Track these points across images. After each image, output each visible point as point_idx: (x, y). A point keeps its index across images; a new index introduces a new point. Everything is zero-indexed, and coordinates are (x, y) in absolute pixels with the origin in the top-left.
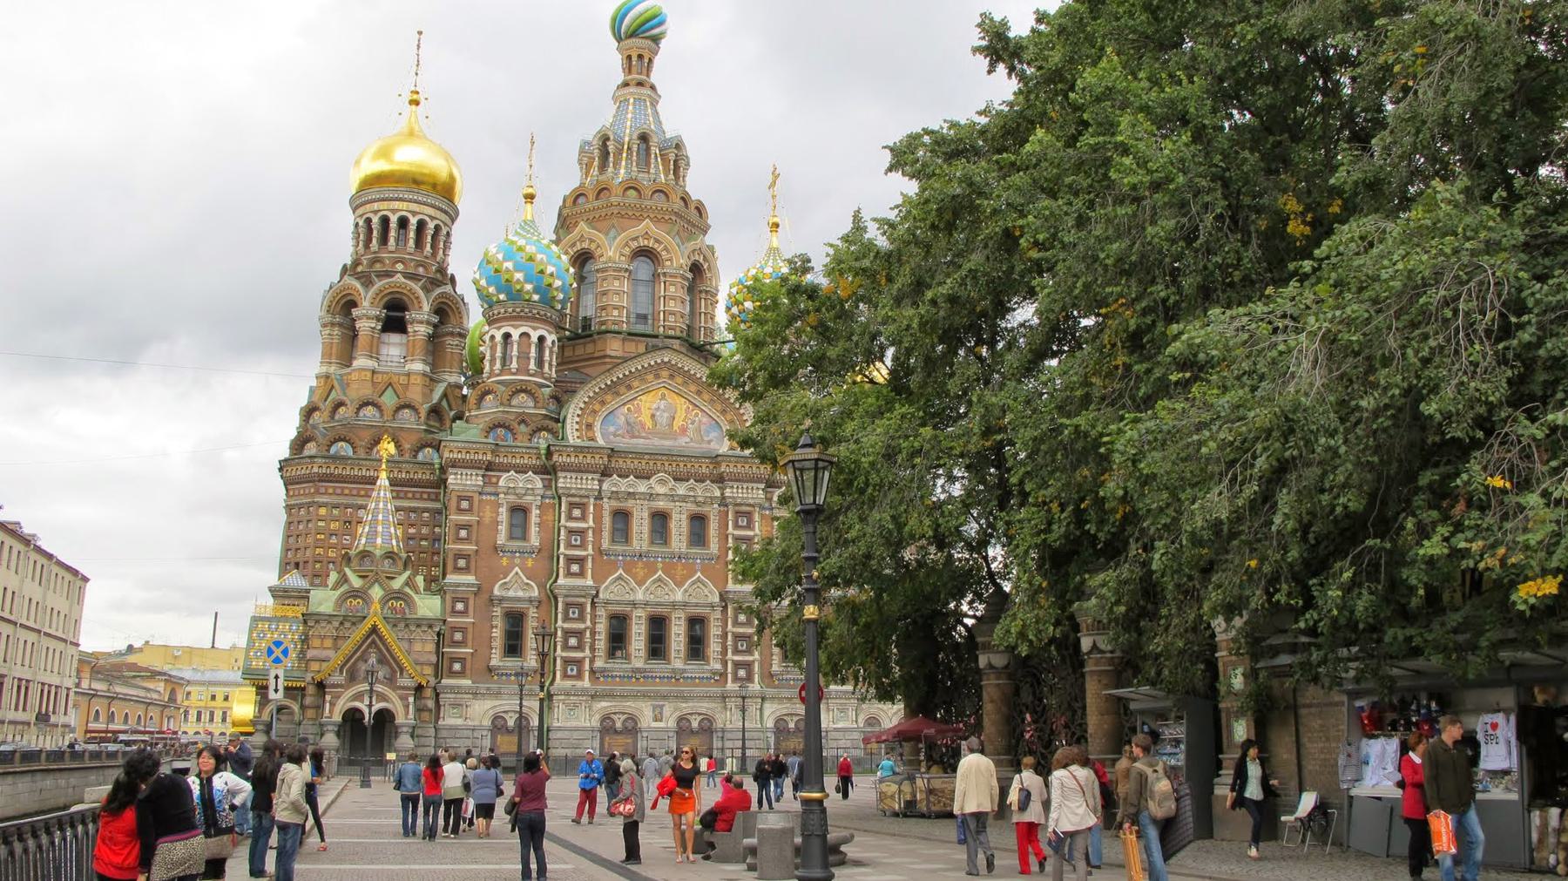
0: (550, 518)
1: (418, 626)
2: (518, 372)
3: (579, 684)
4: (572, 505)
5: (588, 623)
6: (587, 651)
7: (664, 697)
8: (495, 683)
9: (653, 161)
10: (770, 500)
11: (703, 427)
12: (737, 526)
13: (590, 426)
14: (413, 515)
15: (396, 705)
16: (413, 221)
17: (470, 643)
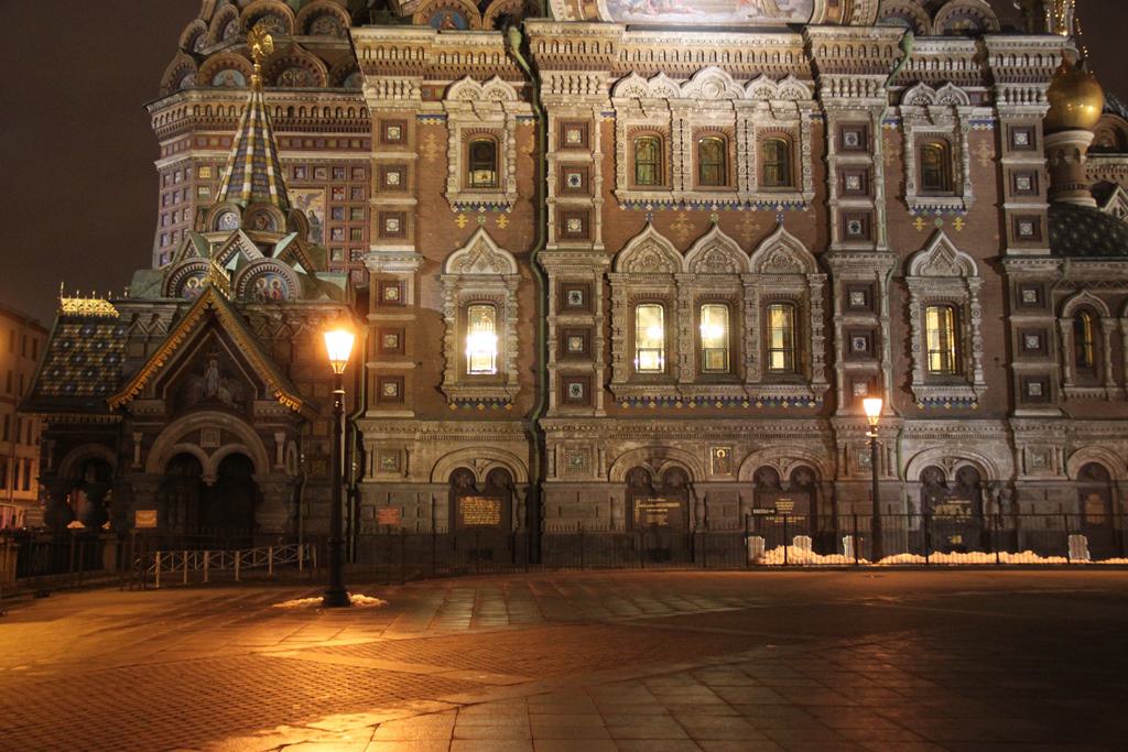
5: (600, 313)
12: (842, 148)
15: (252, 444)
17: (410, 352)
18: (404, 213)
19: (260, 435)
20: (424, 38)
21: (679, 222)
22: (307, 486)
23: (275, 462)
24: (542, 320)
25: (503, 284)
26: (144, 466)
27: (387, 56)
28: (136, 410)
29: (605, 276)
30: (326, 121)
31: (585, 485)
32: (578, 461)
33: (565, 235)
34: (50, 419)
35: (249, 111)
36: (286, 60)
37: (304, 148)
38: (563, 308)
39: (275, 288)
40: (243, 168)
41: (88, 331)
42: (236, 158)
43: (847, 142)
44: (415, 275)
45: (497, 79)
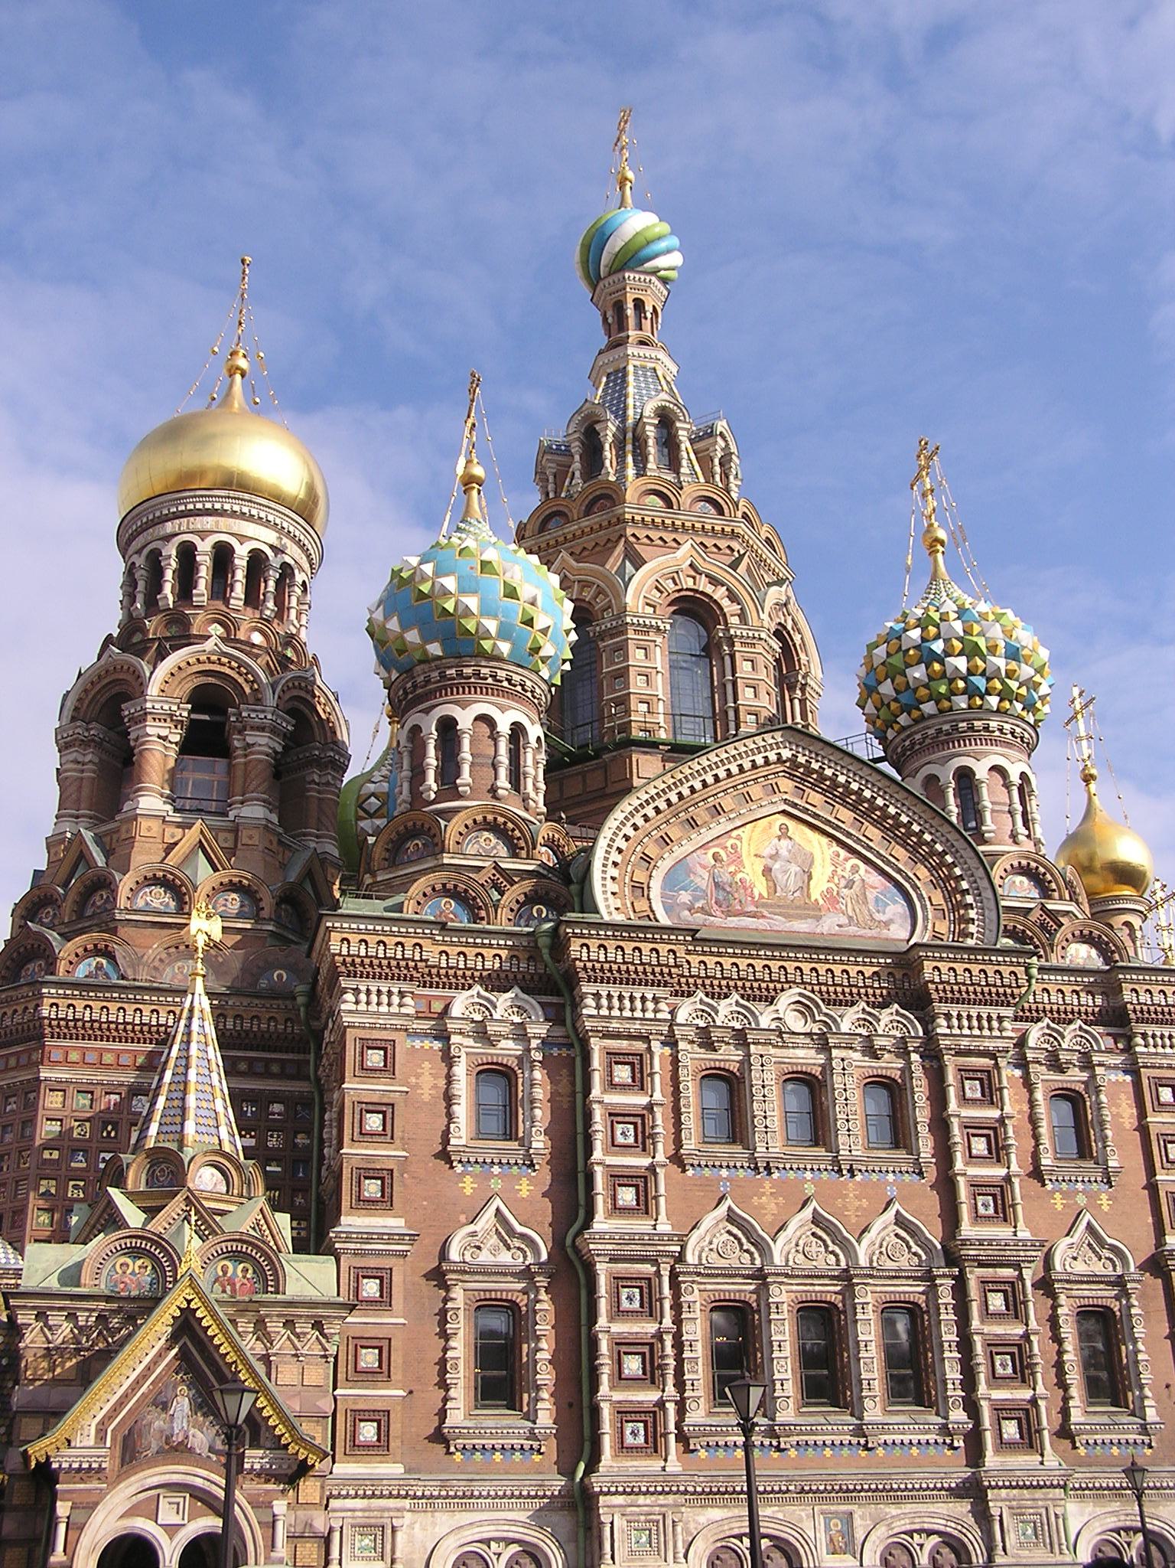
0: (564, 1087)
1: (289, 1324)
2: (474, 794)
3: (656, 1465)
4: (614, 1058)
5: (668, 1322)
6: (670, 1389)
7: (848, 1493)
8: (460, 1468)
9: (684, 454)
10: (1021, 1042)
11: (871, 895)
12: (964, 1100)
13: (640, 889)
14: (249, 1110)
16: (242, 552)
17: (396, 1375)
18: (392, 1170)
21: (763, 1194)
23: (273, 1546)
24: (584, 1330)
29: (673, 1268)
35: (190, 1018)
39: (244, 1277)
43: (969, 1094)
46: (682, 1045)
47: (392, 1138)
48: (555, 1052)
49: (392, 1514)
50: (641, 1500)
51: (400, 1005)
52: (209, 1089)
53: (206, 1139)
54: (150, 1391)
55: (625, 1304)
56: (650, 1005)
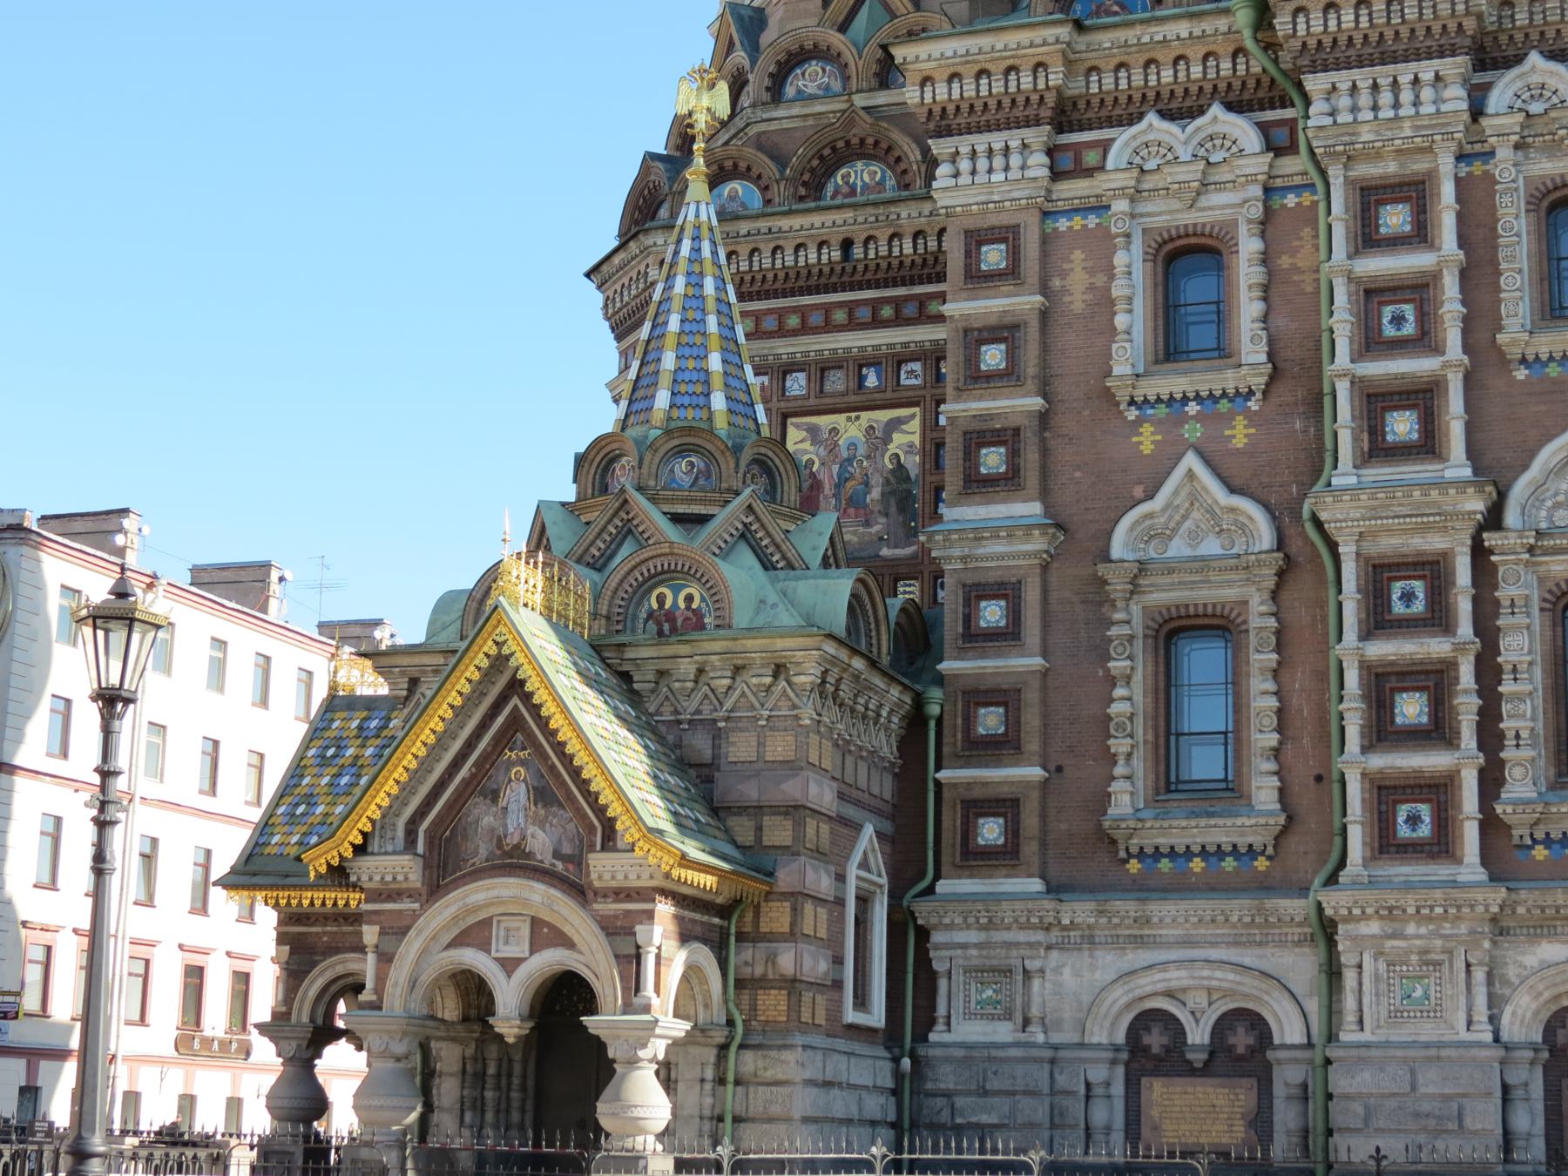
3: (1441, 871)
4: (1370, 197)
5: (1465, 629)
17: (1032, 744)
18: (1017, 431)
19: (603, 928)
20: (1045, 43)
22: (741, 1047)
25: (1243, 575)
26: (381, 999)
27: (970, 92)
28: (365, 878)
30: (919, 261)
31: (1432, 1052)
32: (1419, 993)
33: (1377, 449)
34: (283, 902)
35: (679, 241)
36: (840, 144)
37: (877, 323)
38: (1378, 621)
39: (688, 608)
40: (659, 360)
41: (374, 724)
42: (648, 342)
44: (1045, 568)
45: (1216, 110)
46: (1504, 153)
47: (1018, 379)
48: (1291, 200)
49: (1022, 952)
50: (1411, 929)
51: (1023, 167)
52: (698, 340)
53: (690, 414)
54: (473, 776)
55: (1398, 608)
56: (1427, 94)
